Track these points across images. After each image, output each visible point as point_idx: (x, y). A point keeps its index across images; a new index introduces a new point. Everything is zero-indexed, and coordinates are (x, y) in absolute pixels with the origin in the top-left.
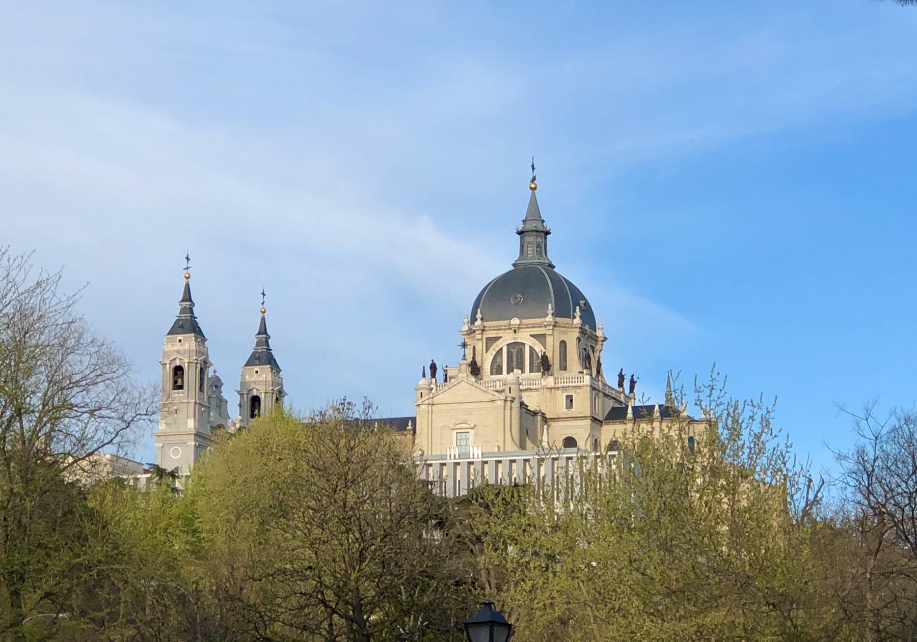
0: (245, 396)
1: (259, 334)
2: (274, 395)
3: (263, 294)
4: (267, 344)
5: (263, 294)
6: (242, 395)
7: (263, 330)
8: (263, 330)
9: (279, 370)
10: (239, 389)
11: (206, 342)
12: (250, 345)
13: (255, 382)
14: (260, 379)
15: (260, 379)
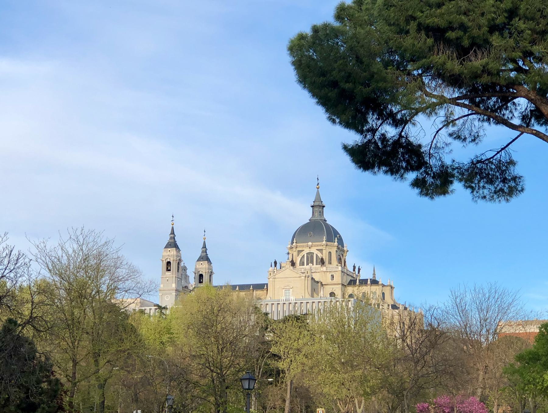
0: (197, 274)
1: (202, 248)
2: (209, 274)
3: (205, 231)
4: (206, 252)
5: (205, 231)
6: (195, 273)
7: (204, 247)
8: (204, 247)
9: (211, 263)
10: (194, 271)
11: (180, 252)
12: (199, 253)
13: (201, 268)
14: (203, 267)
15: (203, 267)
